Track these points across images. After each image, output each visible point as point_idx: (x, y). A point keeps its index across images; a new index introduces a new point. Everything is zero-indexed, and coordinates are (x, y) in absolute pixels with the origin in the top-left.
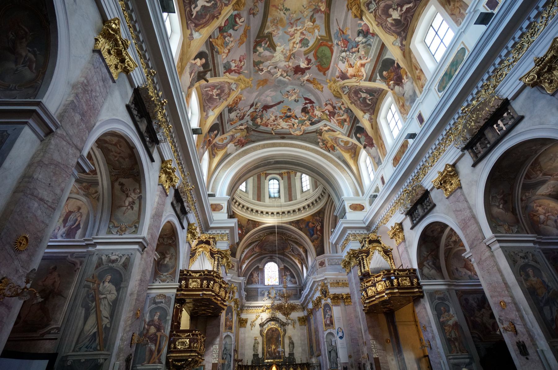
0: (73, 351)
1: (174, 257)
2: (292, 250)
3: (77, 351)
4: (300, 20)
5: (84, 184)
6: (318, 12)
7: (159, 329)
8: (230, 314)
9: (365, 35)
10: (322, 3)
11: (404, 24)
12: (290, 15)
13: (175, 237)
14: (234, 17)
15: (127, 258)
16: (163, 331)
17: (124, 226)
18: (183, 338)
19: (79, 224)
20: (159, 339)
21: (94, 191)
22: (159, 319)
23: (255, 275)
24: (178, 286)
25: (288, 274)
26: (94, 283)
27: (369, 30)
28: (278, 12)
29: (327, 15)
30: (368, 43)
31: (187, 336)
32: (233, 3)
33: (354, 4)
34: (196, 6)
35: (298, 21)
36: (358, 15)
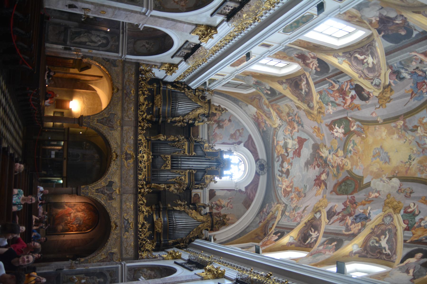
4: (418, 141)
6: (406, 127)
9: (398, 73)
10: (397, 125)
11: (371, 48)
12: (414, 154)
14: (406, 214)
27: (390, 73)
28: (412, 167)
29: (406, 117)
30: (401, 66)
32: (393, 213)
33: (384, 97)
34: (385, 248)
35: (420, 143)
36: (389, 89)
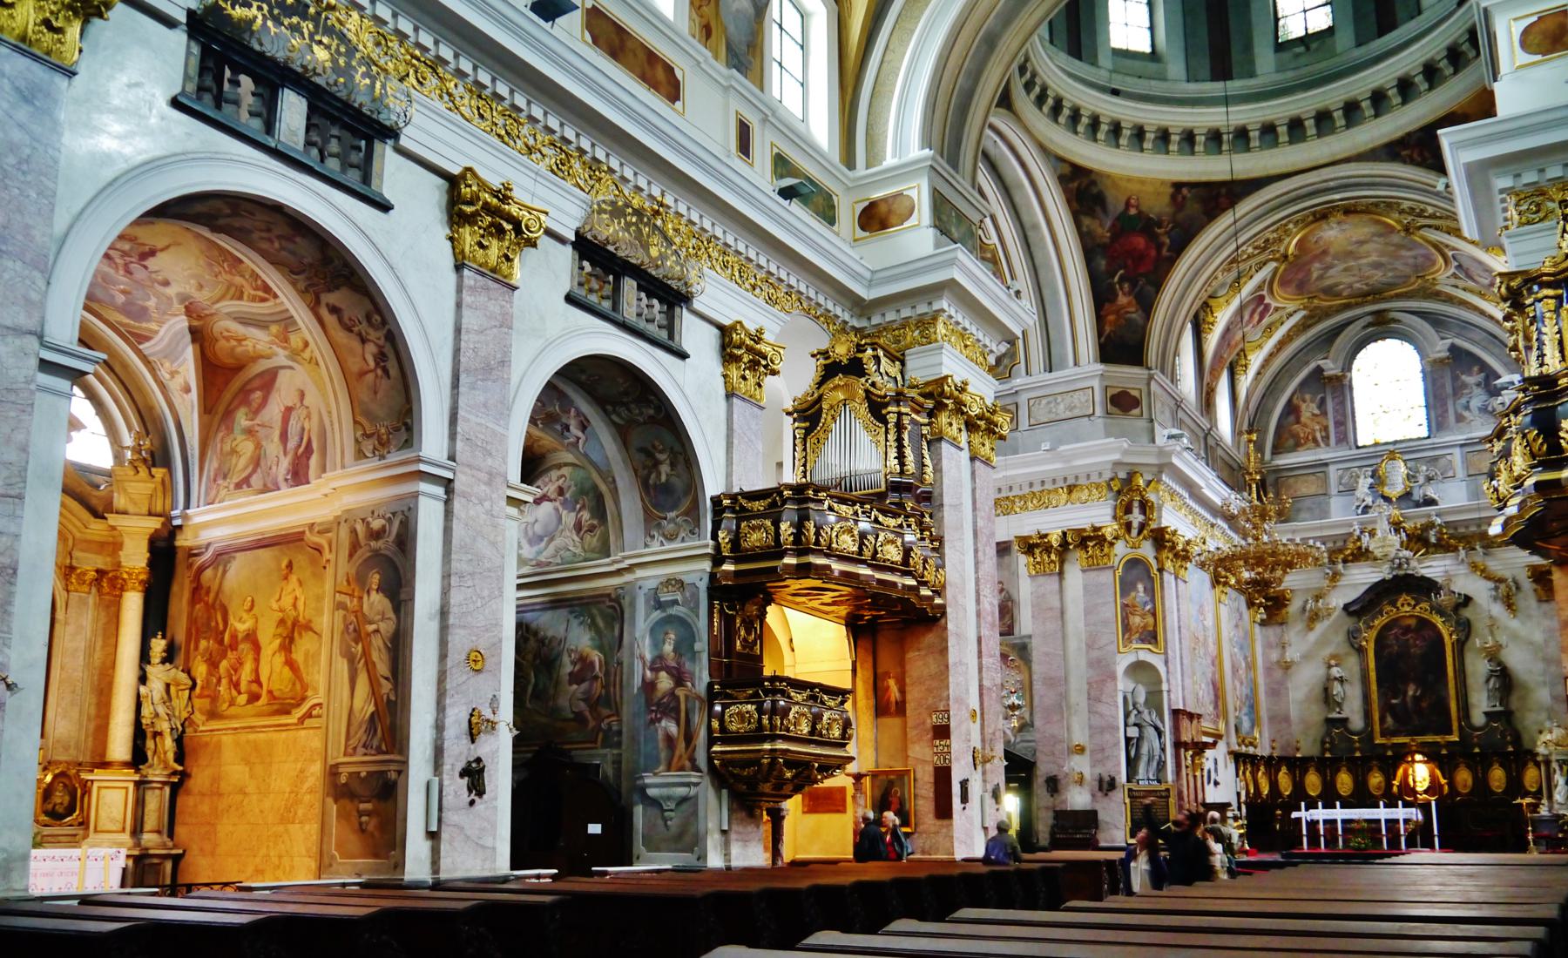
0: (345, 754)
1: (681, 458)
2: (1459, 267)
3: (351, 755)
5: (274, 329)
7: (679, 678)
8: (1140, 587)
13: (655, 395)
15: (401, 522)
16: (689, 684)
17: (383, 431)
18: (741, 703)
19: (309, 441)
20: (683, 707)
21: (301, 345)
22: (675, 650)
23: (1308, 409)
24: (710, 551)
25: (1471, 380)
26: (351, 596)
31: (751, 696)
